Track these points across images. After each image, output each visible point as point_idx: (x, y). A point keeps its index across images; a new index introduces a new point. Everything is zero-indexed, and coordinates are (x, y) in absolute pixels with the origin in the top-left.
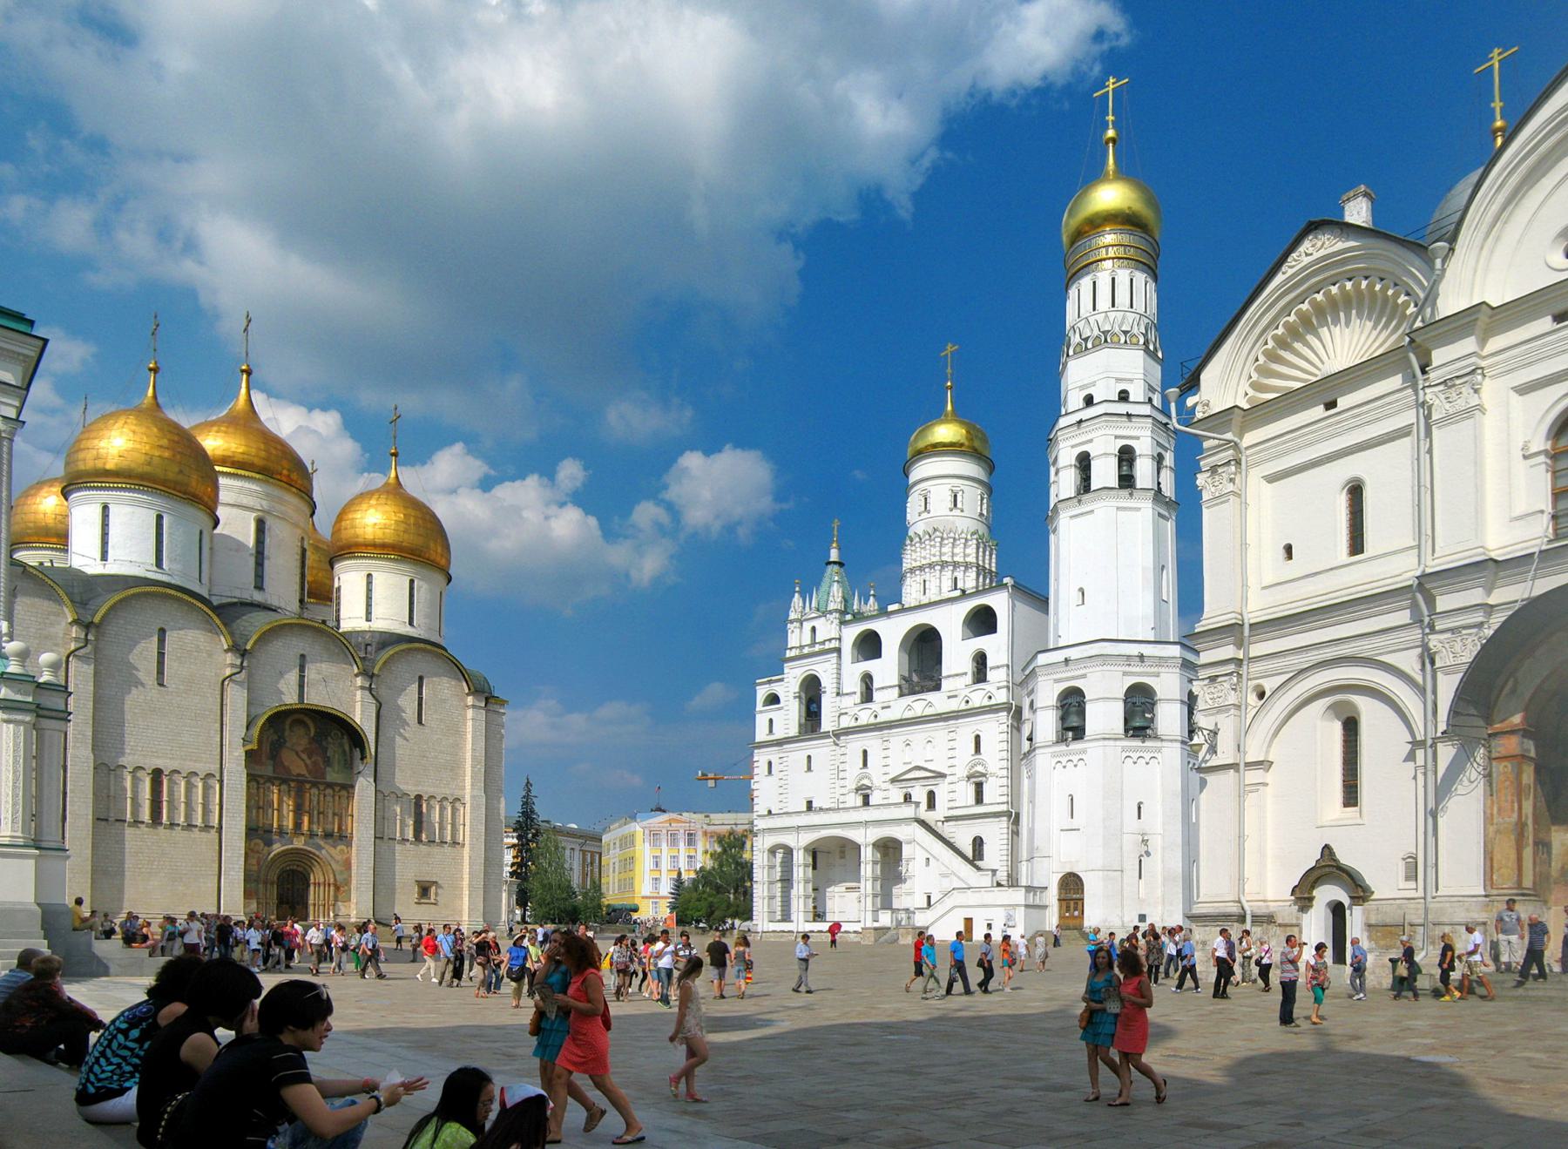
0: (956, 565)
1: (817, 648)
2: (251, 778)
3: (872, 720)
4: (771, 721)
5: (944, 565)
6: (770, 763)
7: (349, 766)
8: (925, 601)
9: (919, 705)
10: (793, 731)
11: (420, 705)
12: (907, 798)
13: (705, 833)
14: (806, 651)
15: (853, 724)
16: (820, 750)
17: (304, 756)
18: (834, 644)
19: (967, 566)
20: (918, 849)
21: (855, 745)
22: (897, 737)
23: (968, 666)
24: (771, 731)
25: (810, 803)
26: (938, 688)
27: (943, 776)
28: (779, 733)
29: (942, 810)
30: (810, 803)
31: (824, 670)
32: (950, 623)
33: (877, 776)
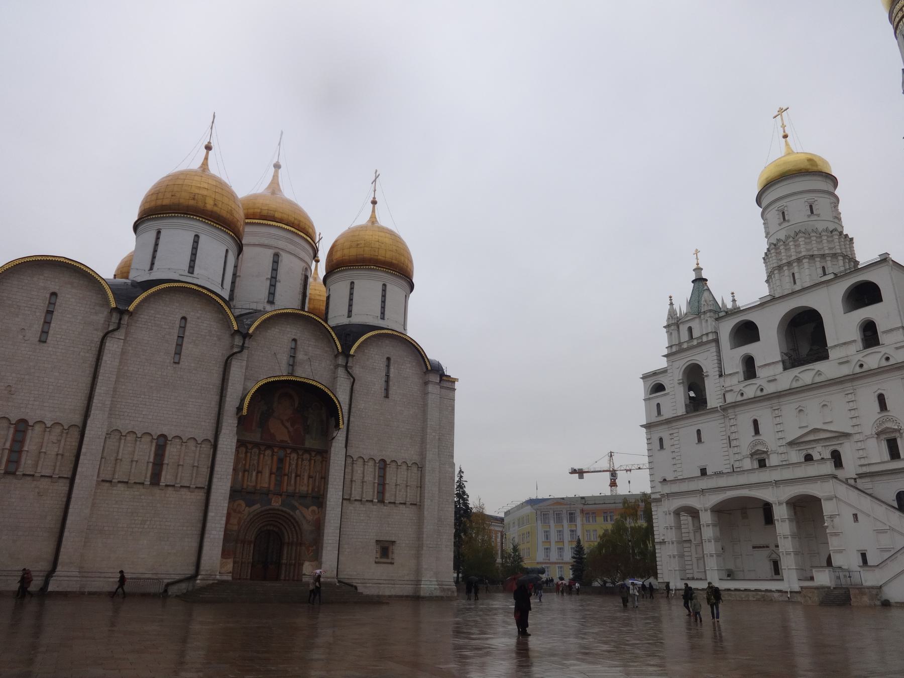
0: (823, 256)
1: (695, 342)
2: (241, 444)
3: (759, 393)
4: (658, 405)
5: (812, 257)
6: (661, 440)
7: (327, 437)
8: (798, 287)
9: (806, 374)
10: (681, 411)
11: (387, 382)
12: (809, 458)
13: (582, 511)
14: (685, 346)
15: (739, 398)
16: (710, 425)
17: (288, 424)
18: (711, 337)
19: (834, 256)
20: (839, 504)
21: (744, 420)
22: (789, 408)
23: (856, 335)
24: (659, 413)
25: (703, 472)
26: (826, 357)
27: (846, 435)
28: (667, 413)
29: (850, 468)
30: (703, 472)
31: (706, 360)
32: (829, 303)
33: (769, 438)
